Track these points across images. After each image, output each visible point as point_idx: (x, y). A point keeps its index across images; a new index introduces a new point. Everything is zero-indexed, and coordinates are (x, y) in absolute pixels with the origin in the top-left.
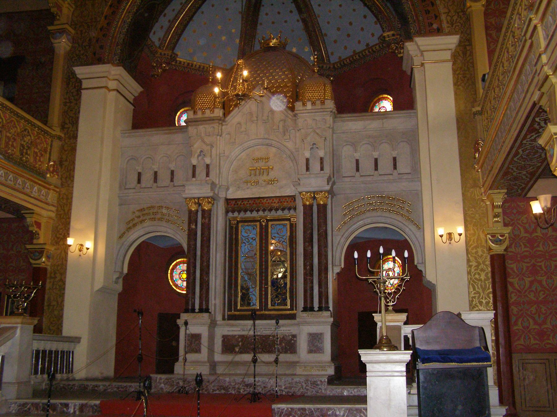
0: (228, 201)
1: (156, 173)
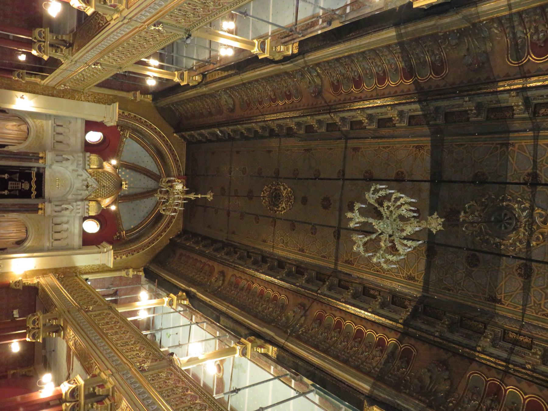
0: (44, 168)
1: (61, 134)
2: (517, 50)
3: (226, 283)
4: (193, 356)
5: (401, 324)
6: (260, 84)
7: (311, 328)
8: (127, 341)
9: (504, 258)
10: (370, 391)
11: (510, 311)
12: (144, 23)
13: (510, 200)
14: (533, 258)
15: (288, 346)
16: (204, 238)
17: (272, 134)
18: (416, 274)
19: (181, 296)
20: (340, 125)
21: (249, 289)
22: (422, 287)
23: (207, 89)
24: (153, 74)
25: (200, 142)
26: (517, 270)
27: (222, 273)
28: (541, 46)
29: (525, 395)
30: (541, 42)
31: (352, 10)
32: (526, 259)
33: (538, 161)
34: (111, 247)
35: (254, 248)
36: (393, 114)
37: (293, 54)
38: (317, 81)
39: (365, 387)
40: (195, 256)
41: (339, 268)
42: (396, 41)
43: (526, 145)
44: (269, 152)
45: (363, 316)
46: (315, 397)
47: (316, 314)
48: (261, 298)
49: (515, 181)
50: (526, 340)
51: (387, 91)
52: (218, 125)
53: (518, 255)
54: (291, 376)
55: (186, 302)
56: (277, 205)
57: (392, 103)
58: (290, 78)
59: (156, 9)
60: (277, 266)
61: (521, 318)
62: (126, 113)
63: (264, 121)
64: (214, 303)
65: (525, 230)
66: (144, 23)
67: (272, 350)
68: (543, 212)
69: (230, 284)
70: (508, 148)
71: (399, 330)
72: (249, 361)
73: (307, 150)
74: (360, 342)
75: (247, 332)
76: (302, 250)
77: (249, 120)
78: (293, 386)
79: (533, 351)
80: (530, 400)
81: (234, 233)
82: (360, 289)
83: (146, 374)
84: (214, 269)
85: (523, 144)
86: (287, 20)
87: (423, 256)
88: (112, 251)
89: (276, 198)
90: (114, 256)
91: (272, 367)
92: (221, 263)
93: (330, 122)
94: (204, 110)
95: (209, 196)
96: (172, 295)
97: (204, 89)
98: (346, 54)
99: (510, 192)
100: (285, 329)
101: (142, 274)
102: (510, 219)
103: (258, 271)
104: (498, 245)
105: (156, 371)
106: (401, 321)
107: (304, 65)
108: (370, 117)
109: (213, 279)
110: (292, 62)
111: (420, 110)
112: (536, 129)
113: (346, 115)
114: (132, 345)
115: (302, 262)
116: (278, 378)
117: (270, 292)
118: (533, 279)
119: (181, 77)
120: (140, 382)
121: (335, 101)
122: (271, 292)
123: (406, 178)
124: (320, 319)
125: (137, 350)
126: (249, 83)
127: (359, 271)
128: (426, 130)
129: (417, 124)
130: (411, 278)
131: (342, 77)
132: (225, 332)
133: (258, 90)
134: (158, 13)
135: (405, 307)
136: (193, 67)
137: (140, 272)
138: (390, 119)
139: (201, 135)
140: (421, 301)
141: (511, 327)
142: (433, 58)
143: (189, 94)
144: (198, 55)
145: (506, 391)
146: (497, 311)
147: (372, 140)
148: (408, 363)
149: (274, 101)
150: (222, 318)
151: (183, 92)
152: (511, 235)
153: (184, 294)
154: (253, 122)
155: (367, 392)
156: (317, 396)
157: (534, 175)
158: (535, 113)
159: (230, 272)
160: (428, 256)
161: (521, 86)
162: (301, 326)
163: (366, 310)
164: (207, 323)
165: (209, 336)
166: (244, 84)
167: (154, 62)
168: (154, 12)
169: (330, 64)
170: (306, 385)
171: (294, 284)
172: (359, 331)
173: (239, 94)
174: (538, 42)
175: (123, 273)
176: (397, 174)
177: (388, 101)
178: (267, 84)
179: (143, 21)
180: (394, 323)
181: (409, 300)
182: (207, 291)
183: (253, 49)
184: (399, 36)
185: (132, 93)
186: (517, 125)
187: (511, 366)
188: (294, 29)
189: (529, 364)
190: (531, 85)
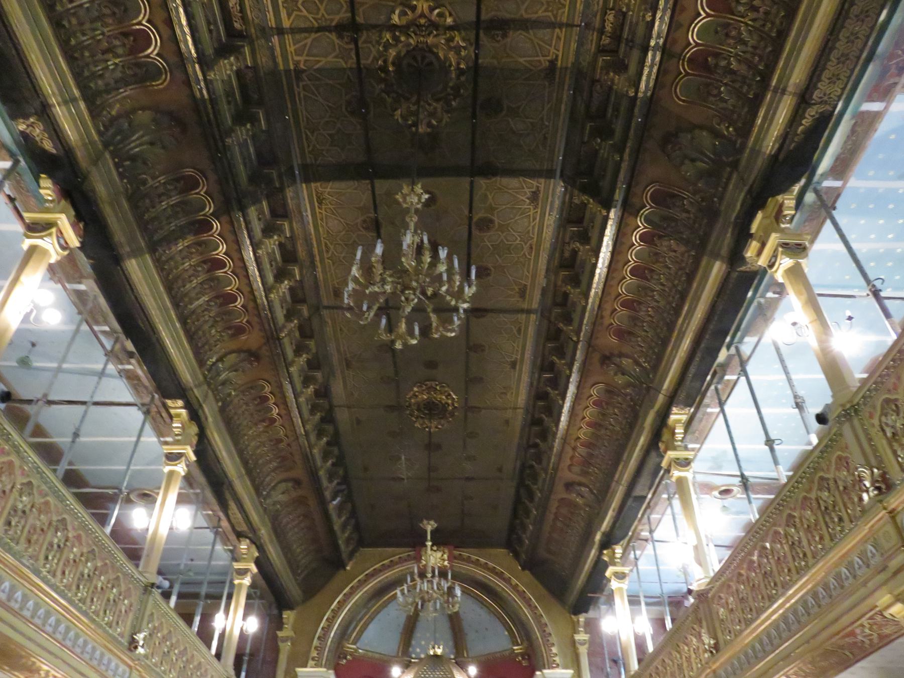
2: (144, 74)
3: (583, 479)
4: (691, 554)
5: (608, 212)
6: (249, 445)
7: (639, 348)
8: (676, 666)
9: (480, 61)
10: (723, 261)
11: (567, 43)
12: (130, 667)
13: (385, 61)
14: (474, 19)
15: (668, 388)
16: (515, 514)
17: (329, 418)
18: (527, 190)
19: (609, 557)
20: (299, 320)
21: (588, 445)
22: (548, 181)
23: (262, 528)
24: (237, 622)
25: (357, 528)
26: (498, 42)
27: (569, 486)
28: (134, 40)
29: (700, 15)
30: (126, 41)
31: (106, 322)
33: (316, 25)
34: (538, 673)
35: (521, 437)
36: (271, 244)
37: (185, 407)
38: (232, 358)
39: (718, 269)
40: (547, 528)
41: (535, 305)
42: (148, 256)
43: (294, 44)
44: (359, 422)
45: (605, 270)
46: (747, 344)
47: (614, 340)
48: (600, 425)
49: (354, 56)
50: (611, 17)
51: (236, 256)
52: (323, 503)
53: (473, 40)
54: (718, 383)
55: (619, 550)
56: (444, 405)
57: (251, 249)
58: (231, 401)
59: (102, 655)
60: (544, 403)
61: (575, 28)
62: (314, 654)
63: (307, 434)
64: (615, 504)
65: (429, 35)
66: (130, 667)
67: (678, 416)
68: (397, 12)
69: (584, 473)
70: (303, 71)
71: (620, 214)
72: (704, 446)
73: (348, 365)
74: (652, 271)
75: (653, 454)
76: (513, 365)
77: (308, 460)
78: (735, 377)
79: (624, 10)
80: (708, 7)
81: (500, 470)
82: (563, 273)
83: (721, 642)
84: (562, 499)
85: (293, 49)
86: (135, 416)
88: (545, 671)
89: (432, 409)
90: (553, 668)
91: (709, 410)
92: (551, 491)
93: (297, 334)
94: (302, 525)
95: (429, 526)
96: (608, 574)
97: (264, 533)
98: (178, 325)
99: (373, 61)
100: (645, 387)
101: (582, 618)
102: (414, 58)
103: (555, 434)
104: (461, 72)
105: (717, 625)
106: (604, 213)
107: (205, 387)
108: (280, 275)
109: (579, 500)
110: (201, 406)
111: (258, 206)
112: (264, 32)
113: (280, 314)
114: (681, 658)
115: (534, 363)
116: (721, 404)
117: (590, 413)
118: (508, 16)
119: (242, 573)
120: (730, 658)
121: (260, 330)
122: (590, 410)
123: (372, 215)
124: (621, 334)
125: (689, 650)
126: (245, 463)
127: (534, 276)
128: (289, 193)
129: (285, 205)
130: (534, 197)
131: (220, 324)
132: (661, 488)
133: (258, 447)
134: (110, 650)
135: (584, 205)
136: (231, 551)
137: (578, 621)
138: (281, 245)
139: (344, 527)
140: (570, 180)
141: (592, 41)
142: (173, 193)
143: (274, 555)
144: (207, 545)
145: (697, 44)
146: (570, 65)
147: (319, 269)
148: (673, 196)
149: (273, 421)
150: (638, 491)
151: (272, 565)
152: (441, 55)
153: (605, 552)
154: (311, 452)
155: (724, 267)
156: (747, 339)
157: (340, 29)
158: (240, 35)
159: (566, 475)
161: (197, 66)
162: (637, 363)
163: (595, 266)
164: (650, 514)
165: (669, 511)
166: (249, 472)
167: (219, 622)
168: (108, 655)
169: (200, 345)
170: (730, 358)
171: (569, 377)
172: (632, 272)
173: (268, 475)
174: (128, 46)
175: (583, 650)
176: (366, 229)
177: (249, 254)
178: (245, 435)
179: (128, 669)
180: (610, 222)
181: (571, 198)
182: (598, 514)
183: (178, 473)
184: (136, 253)
185: (281, 645)
186: (263, 60)
187: (652, 43)
188: (145, 409)
189: (644, 16)
190: (193, 51)
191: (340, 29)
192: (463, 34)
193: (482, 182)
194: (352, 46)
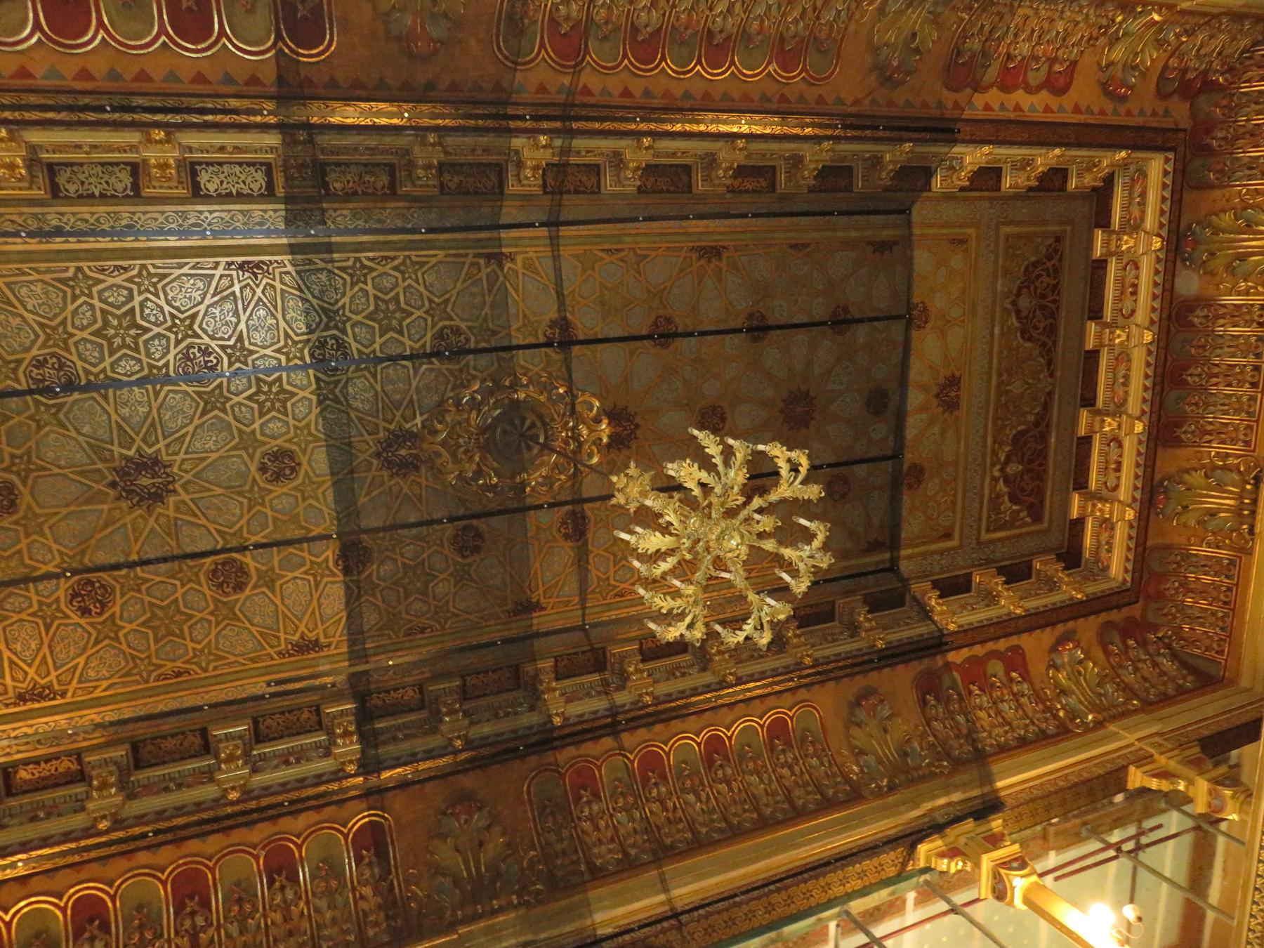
14: (586, 495)
32: (573, 502)
33: (565, 292)
49: (526, 342)
70: (501, 267)
87: (334, 575)
106: (351, 768)
118: (590, 535)
147: (34, 245)
157: (563, 324)
160: (347, 571)
191: (563, 324)
192: (569, 484)
193: (329, 553)
194: (542, 340)
